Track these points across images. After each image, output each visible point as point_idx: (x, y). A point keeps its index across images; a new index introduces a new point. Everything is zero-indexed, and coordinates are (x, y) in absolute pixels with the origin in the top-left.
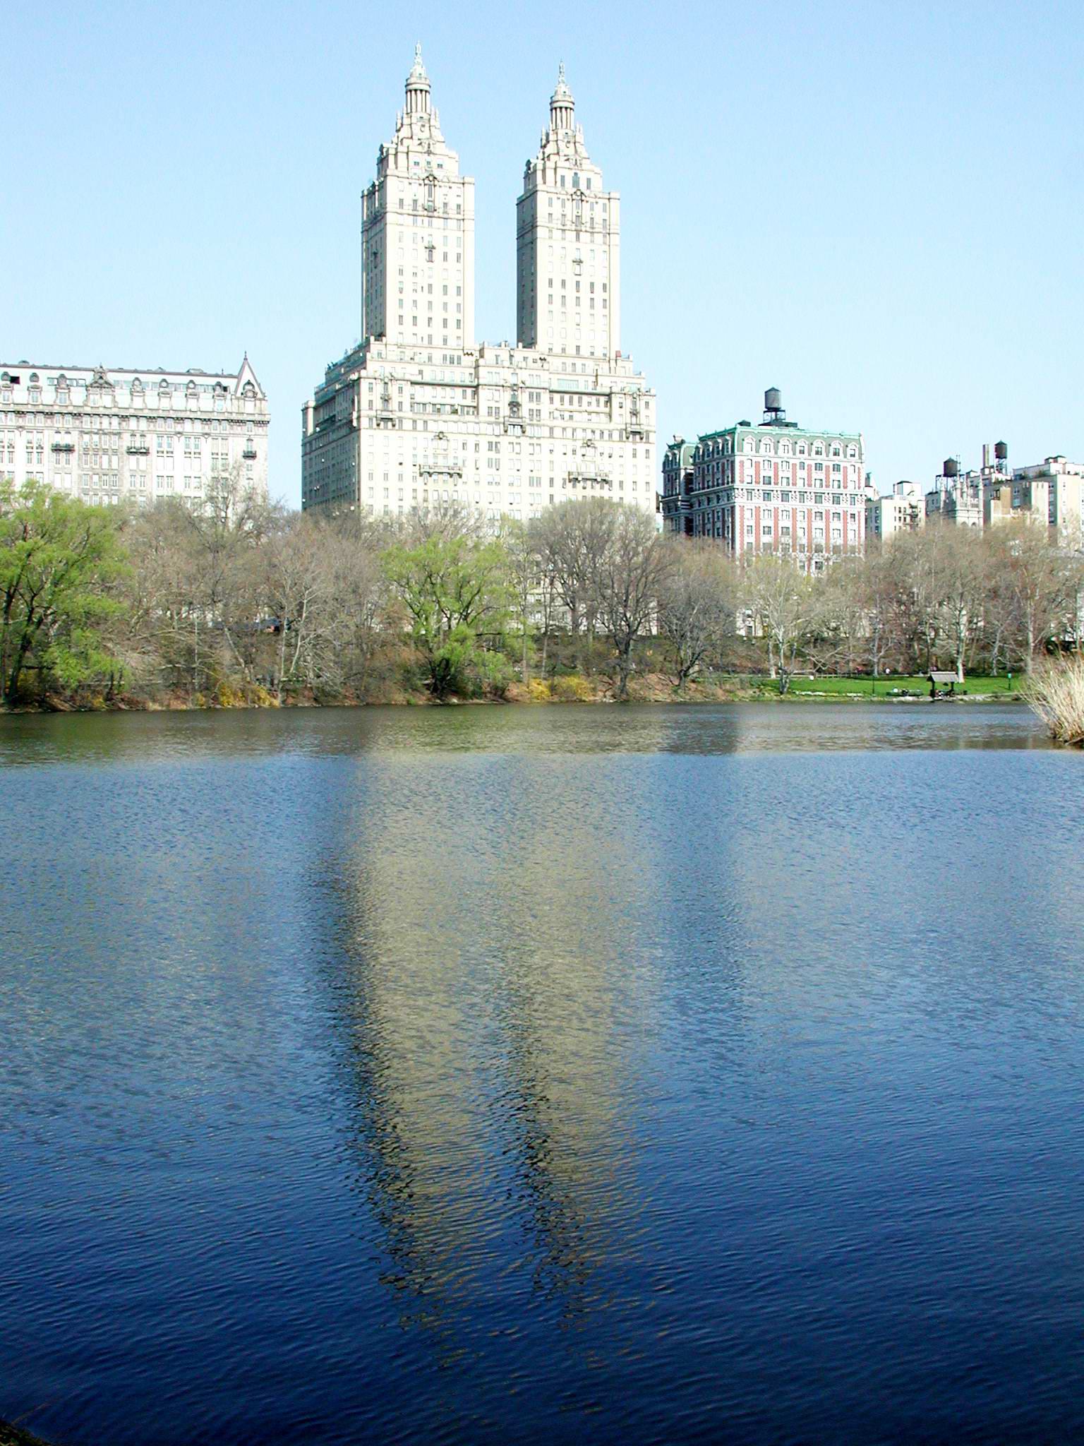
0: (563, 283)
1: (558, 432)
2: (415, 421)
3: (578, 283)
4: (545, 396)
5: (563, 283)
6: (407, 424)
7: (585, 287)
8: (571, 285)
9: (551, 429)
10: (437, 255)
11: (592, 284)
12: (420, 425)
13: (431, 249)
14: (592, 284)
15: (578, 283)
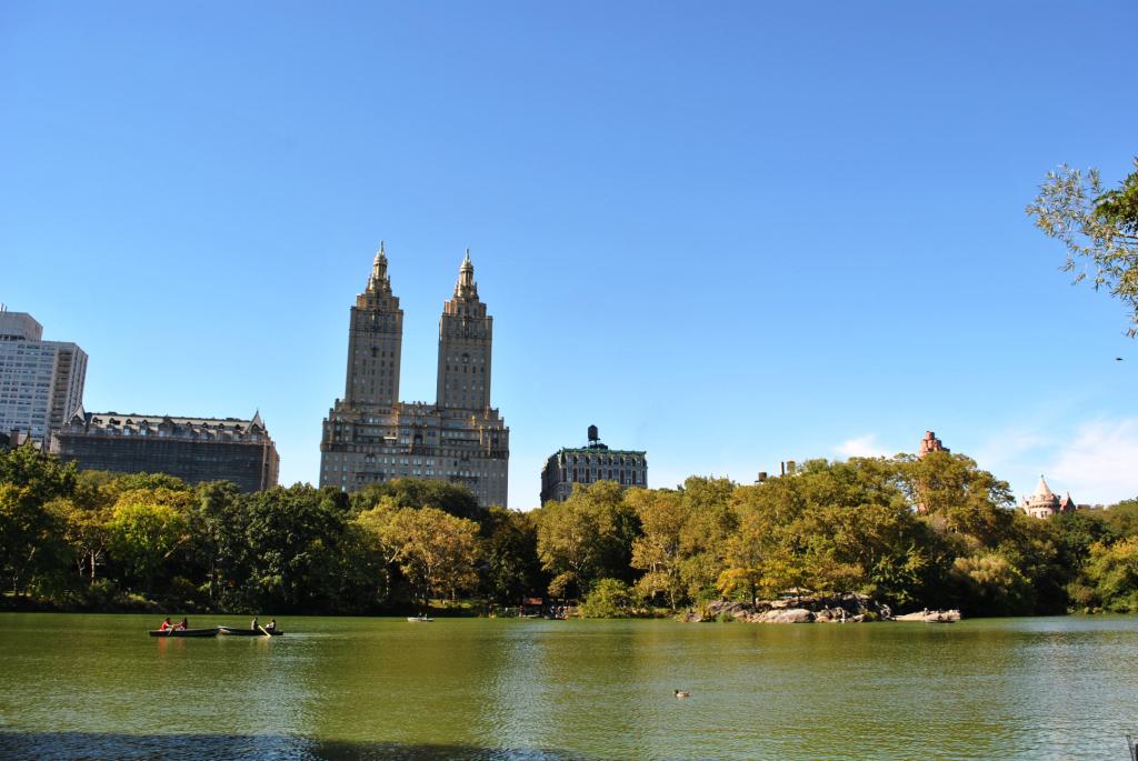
0: (456, 369)
1: (445, 452)
2: (355, 447)
3: (465, 368)
4: (438, 433)
5: (456, 369)
6: (350, 448)
7: (469, 369)
8: (461, 369)
9: (441, 451)
10: (379, 354)
11: (474, 368)
12: (358, 449)
13: (375, 350)
14: (474, 368)
15: (465, 368)
